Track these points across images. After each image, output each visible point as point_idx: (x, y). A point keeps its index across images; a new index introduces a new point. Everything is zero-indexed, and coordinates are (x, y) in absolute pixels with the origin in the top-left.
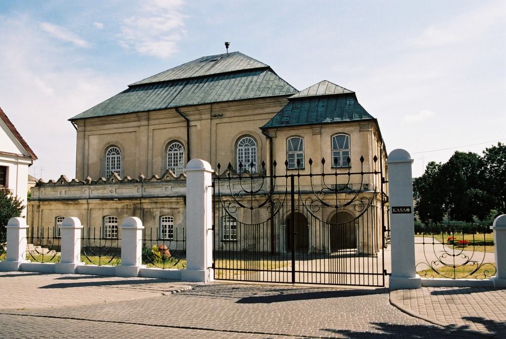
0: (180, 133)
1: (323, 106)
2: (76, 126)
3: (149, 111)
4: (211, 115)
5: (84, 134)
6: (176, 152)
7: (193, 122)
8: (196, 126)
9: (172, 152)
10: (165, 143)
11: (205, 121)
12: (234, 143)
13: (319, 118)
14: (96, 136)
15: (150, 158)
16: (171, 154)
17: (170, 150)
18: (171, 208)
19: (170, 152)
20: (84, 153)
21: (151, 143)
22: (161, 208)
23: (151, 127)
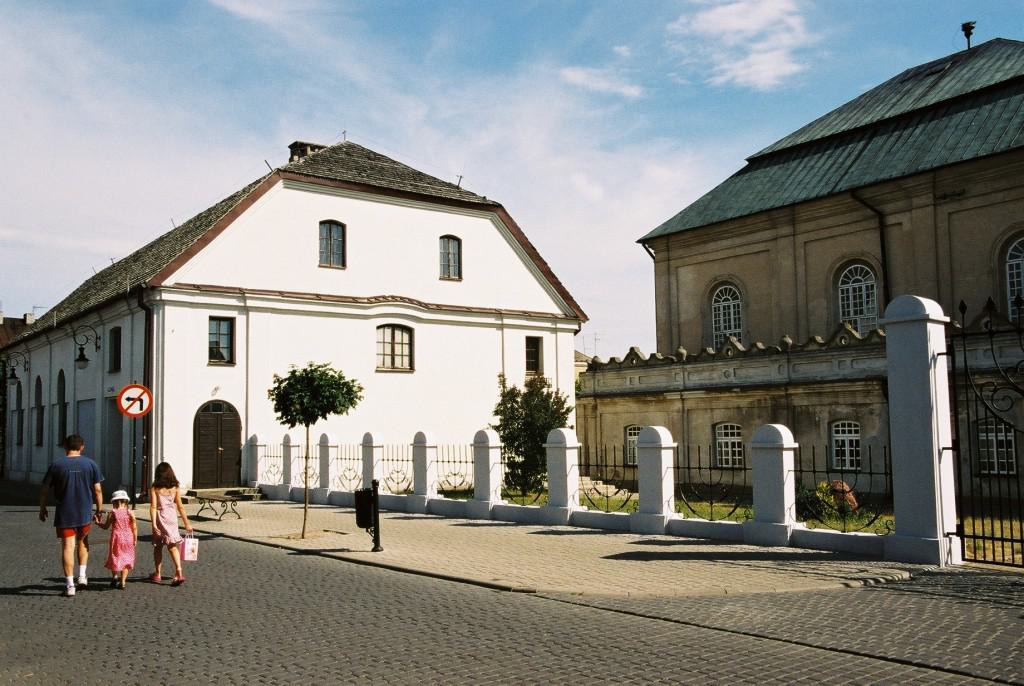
2: (652, 251)
3: (794, 205)
4: (935, 196)
6: (856, 285)
8: (900, 224)
9: (850, 286)
10: (831, 268)
11: (920, 211)
14: (691, 267)
15: (801, 302)
17: (844, 283)
18: (852, 405)
19: (845, 287)
20: (669, 303)
21: (801, 270)
22: (830, 404)
23: (801, 239)
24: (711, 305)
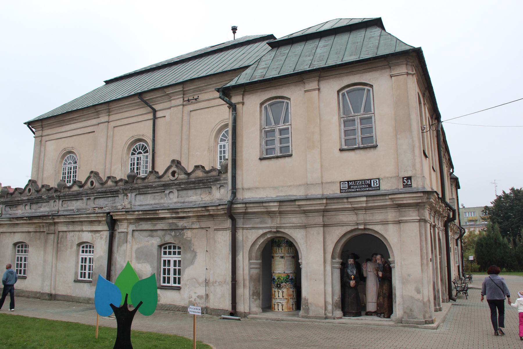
0: (144, 130)
1: (324, 46)
2: (34, 130)
5: (41, 141)
8: (165, 116)
9: (136, 156)
11: (175, 109)
12: (213, 136)
13: (316, 63)
15: (108, 166)
16: (134, 158)
17: (133, 154)
19: (133, 156)
21: (110, 144)
22: (79, 231)
23: (112, 124)
24: (61, 167)
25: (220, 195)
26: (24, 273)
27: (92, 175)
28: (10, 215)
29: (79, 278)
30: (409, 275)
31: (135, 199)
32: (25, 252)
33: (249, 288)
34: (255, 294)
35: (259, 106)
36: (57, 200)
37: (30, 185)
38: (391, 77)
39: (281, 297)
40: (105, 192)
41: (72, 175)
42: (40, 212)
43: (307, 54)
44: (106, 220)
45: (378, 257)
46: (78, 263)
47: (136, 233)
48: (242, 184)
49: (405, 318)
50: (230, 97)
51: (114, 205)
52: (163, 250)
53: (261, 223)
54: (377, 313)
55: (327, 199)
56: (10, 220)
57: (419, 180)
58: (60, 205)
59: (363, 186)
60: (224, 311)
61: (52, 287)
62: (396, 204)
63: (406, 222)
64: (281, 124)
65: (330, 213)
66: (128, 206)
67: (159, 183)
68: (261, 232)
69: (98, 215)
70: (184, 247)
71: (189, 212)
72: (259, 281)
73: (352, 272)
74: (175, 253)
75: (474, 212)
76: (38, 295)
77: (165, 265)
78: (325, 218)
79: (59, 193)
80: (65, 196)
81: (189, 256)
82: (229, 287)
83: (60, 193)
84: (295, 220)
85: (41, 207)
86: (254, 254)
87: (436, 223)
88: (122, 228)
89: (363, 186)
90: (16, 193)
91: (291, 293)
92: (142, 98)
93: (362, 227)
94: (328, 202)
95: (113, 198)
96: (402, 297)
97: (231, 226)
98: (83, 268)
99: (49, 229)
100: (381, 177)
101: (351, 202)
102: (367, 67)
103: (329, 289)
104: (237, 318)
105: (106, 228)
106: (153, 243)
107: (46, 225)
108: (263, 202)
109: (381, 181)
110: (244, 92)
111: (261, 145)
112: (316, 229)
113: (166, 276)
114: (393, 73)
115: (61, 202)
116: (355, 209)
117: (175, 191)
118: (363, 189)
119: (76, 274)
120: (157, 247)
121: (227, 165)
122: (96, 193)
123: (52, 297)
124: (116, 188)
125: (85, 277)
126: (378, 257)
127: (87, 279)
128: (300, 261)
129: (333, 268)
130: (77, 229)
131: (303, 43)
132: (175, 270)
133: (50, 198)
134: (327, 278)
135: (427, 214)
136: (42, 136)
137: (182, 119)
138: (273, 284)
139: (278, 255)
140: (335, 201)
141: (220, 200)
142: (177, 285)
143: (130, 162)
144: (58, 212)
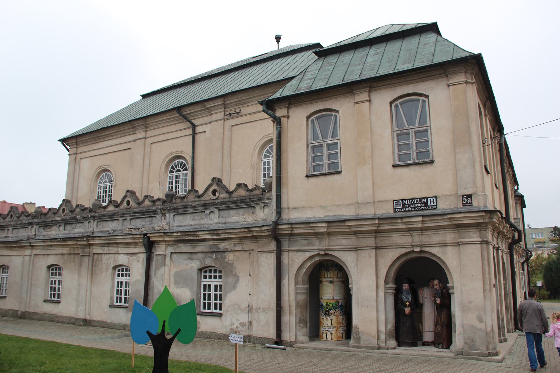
0: (183, 146)
1: (375, 54)
2: (68, 147)
5: (75, 159)
7: (200, 127)
9: (174, 174)
11: (216, 123)
13: (366, 73)
15: (145, 185)
16: (173, 177)
17: (171, 172)
19: (171, 174)
21: (147, 162)
22: (115, 253)
23: (149, 141)
25: (263, 215)
26: (58, 298)
27: (128, 194)
28: (44, 236)
29: (115, 303)
30: (470, 302)
31: (174, 220)
32: (59, 275)
33: (296, 315)
34: (301, 321)
35: (305, 119)
36: (92, 221)
37: (64, 204)
38: (449, 86)
39: (330, 324)
40: (142, 212)
41: (108, 194)
42: (74, 234)
43: (357, 63)
44: (143, 242)
45: (436, 282)
46: (113, 287)
47: (175, 256)
48: (288, 203)
49: (466, 350)
50: (274, 111)
51: (152, 226)
52: (203, 274)
53: (308, 245)
54: (434, 343)
55: (379, 219)
56: (44, 242)
57: (481, 198)
58: (95, 226)
59: (419, 205)
60: (268, 340)
61: (87, 312)
62: (455, 224)
63: (467, 243)
64: (329, 139)
65: (382, 235)
66: (167, 227)
67: (199, 203)
68: (308, 255)
69: (135, 236)
70: (225, 271)
71: (230, 233)
72: (306, 307)
73: (407, 298)
74: (215, 277)
75: (541, 233)
76: (72, 321)
77: (205, 290)
78: (378, 240)
79: (94, 214)
80: (100, 216)
81: (231, 280)
82: (272, 315)
83: (95, 213)
84: (345, 241)
85: (75, 228)
86: (300, 279)
87: (500, 245)
88: (160, 250)
89: (419, 205)
90: (50, 213)
91: (341, 321)
92: (180, 112)
93: (417, 249)
94: (381, 222)
95: (151, 219)
96: (463, 326)
97: (275, 249)
98: (119, 292)
99: (83, 251)
100: (438, 195)
101: (405, 222)
102: (422, 76)
103: (382, 317)
104: (283, 347)
105: (143, 250)
106: (192, 267)
107: (82, 246)
108: (310, 223)
109: (438, 199)
110: (289, 104)
111: (307, 161)
112: (368, 251)
113: (207, 301)
114: (450, 82)
115: (96, 223)
116: (410, 230)
117: (216, 211)
118: (418, 209)
119: (112, 298)
120: (196, 271)
121: (272, 183)
122: (133, 213)
123: (87, 323)
124: (154, 208)
125: (121, 302)
126: (436, 282)
127: (123, 304)
128: (350, 286)
129: (386, 293)
130: (112, 252)
131: (352, 52)
132: (216, 295)
133: (85, 219)
134: (379, 305)
135: (489, 235)
136: (76, 154)
137: (223, 134)
138: (321, 311)
139: (326, 280)
140: (389, 221)
141: (265, 220)
142: (218, 311)
143: (168, 181)
144: (93, 233)
